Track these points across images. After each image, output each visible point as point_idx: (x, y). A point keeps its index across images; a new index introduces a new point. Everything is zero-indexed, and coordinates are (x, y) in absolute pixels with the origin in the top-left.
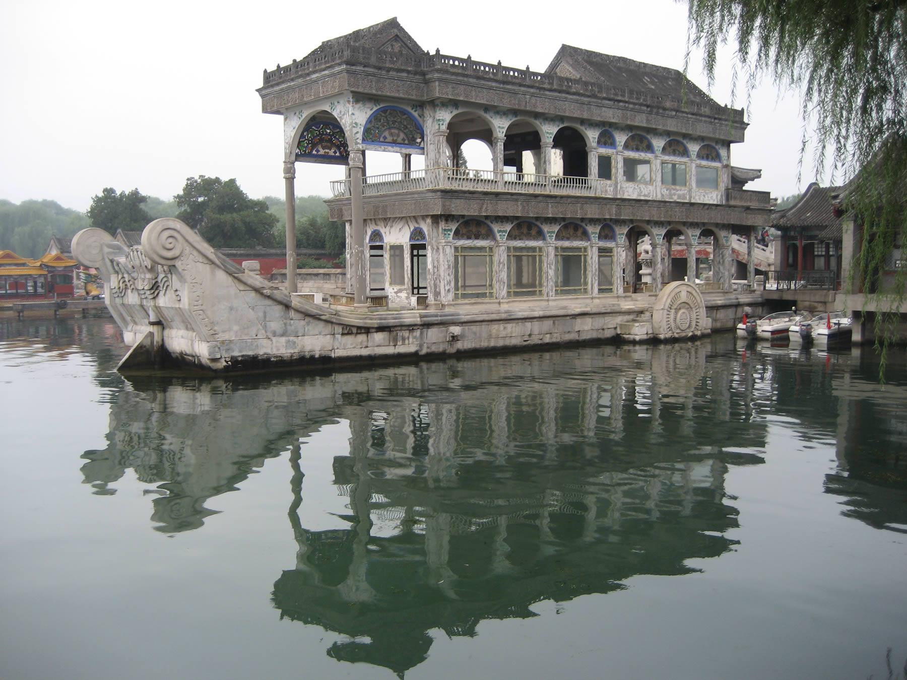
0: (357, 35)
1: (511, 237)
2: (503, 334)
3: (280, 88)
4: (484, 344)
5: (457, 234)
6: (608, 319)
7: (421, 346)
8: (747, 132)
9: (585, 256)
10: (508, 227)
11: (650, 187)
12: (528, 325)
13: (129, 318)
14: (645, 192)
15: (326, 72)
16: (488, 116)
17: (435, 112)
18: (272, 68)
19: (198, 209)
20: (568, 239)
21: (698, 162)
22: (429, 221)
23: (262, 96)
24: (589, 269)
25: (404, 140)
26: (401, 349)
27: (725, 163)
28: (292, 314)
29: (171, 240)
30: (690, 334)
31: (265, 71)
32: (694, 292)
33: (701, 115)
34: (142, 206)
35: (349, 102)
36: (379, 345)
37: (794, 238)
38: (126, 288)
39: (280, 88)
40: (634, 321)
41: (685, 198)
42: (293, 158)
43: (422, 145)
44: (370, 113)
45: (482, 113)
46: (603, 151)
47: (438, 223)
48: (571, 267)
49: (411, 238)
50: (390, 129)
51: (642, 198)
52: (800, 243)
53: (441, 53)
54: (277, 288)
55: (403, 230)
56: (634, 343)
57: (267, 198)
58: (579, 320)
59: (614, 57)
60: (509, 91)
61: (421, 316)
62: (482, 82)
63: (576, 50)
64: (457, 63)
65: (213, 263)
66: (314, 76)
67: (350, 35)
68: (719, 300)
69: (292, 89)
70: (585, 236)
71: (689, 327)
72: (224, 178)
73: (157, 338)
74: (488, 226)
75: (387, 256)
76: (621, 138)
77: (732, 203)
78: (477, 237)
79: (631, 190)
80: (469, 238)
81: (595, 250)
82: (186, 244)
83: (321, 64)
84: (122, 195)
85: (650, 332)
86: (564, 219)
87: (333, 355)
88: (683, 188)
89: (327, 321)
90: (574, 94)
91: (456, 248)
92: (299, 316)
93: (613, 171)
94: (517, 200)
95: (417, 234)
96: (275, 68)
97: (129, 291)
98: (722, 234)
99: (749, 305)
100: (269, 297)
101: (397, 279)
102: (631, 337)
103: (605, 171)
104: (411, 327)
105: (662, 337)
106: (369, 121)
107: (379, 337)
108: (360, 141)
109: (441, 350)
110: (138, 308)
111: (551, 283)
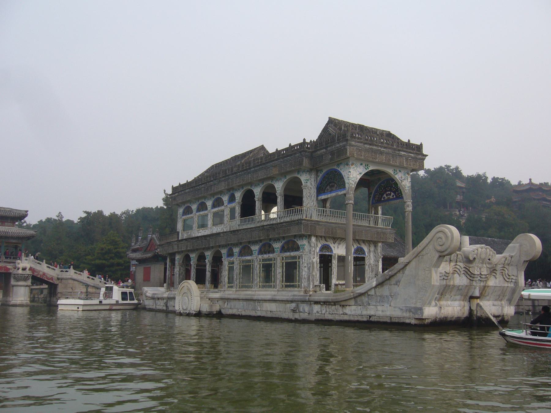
15: (412, 155)
66: (403, 153)
75: (335, 262)
95: (359, 250)
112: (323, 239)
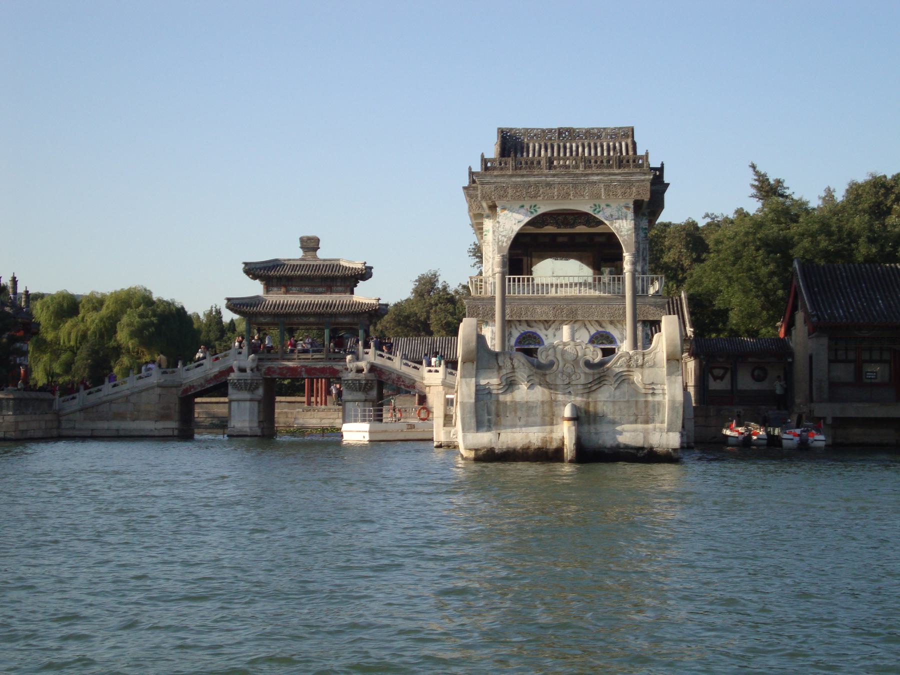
15: (619, 177)
31: (482, 155)
35: (627, 207)
66: (595, 178)
112: (525, 325)
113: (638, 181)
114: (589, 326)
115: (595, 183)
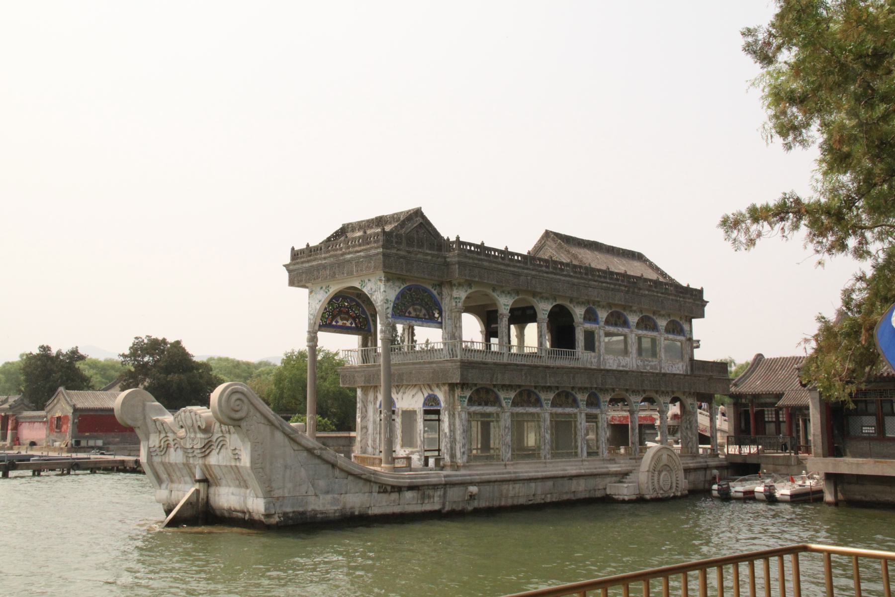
0: (380, 221)
1: (515, 404)
2: (511, 493)
3: (304, 267)
4: (496, 503)
5: (471, 402)
6: (598, 480)
7: (444, 504)
8: (706, 309)
9: (575, 422)
10: (512, 395)
11: (628, 359)
12: (533, 485)
13: (164, 476)
14: (623, 363)
15: (362, 254)
16: (495, 295)
17: (452, 290)
18: (300, 246)
19: (143, 369)
20: (561, 406)
21: (666, 335)
22: (446, 388)
23: (289, 271)
24: (579, 433)
25: (425, 315)
26: (428, 507)
27: (688, 336)
28: (337, 472)
29: (238, 402)
30: (672, 495)
31: (293, 249)
32: (673, 456)
33: (669, 295)
34: (79, 365)
35: (380, 280)
36: (410, 503)
37: (745, 405)
38: (168, 446)
39: (304, 267)
40: (621, 482)
41: (656, 369)
42: (317, 327)
43: (440, 320)
44: (398, 291)
45: (490, 291)
46: (588, 326)
47: (454, 391)
48: (563, 431)
49: (425, 404)
50: (414, 305)
51: (621, 368)
52: (753, 410)
53: (461, 239)
54: (325, 449)
55: (416, 397)
56: (623, 502)
57: (211, 359)
58: (574, 482)
59: (588, 241)
60: (513, 273)
61: (445, 477)
62: (494, 265)
63: (557, 235)
64: (473, 248)
65: (271, 423)
66: (348, 256)
67: (372, 220)
68: (692, 464)
69: (324, 267)
70: (575, 403)
71: (671, 488)
72: (171, 339)
73: (202, 495)
74: (496, 394)
75: (398, 420)
76: (602, 315)
77: (696, 373)
78: (486, 404)
79: (611, 361)
80: (480, 405)
81: (583, 416)
82: (251, 406)
83: (354, 246)
84: (59, 354)
85: (638, 492)
86: (557, 388)
87: (370, 512)
88: (654, 360)
89: (367, 481)
90: (565, 276)
91: (469, 414)
92: (343, 475)
93: (597, 344)
94: (522, 370)
95: (432, 400)
96: (304, 247)
97: (172, 450)
98: (689, 401)
99: (717, 468)
100: (319, 457)
101: (408, 441)
102: (621, 497)
103: (590, 343)
104: (435, 486)
105: (648, 497)
106: (397, 298)
107: (409, 495)
108: (389, 316)
109: (460, 508)
110: (182, 466)
111: (548, 447)
113: (374, 255)
114: (423, 390)
115: (349, 261)
